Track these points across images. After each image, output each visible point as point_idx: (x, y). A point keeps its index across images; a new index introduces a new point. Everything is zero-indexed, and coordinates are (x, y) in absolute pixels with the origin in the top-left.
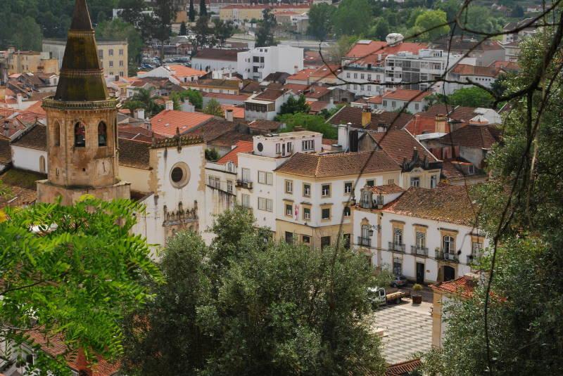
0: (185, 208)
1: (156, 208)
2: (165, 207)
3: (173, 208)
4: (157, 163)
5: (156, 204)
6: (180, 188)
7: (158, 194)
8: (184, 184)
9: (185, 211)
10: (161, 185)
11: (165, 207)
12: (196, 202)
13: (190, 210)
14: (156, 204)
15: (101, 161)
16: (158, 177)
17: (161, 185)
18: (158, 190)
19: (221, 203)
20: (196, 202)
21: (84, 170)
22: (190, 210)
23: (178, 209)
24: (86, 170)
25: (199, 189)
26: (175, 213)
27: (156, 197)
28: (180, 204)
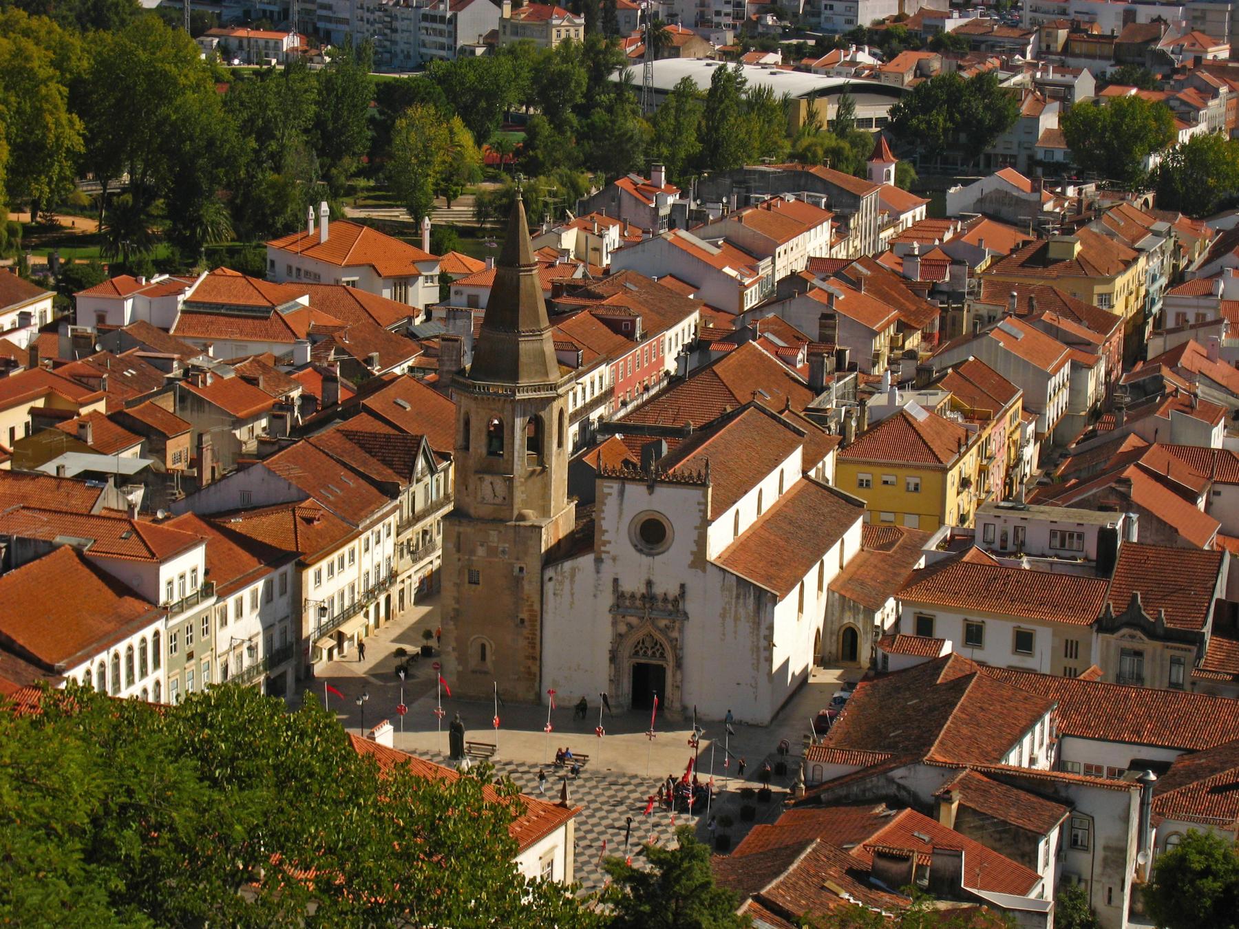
1: (599, 579)
2: (616, 581)
3: (633, 584)
5: (598, 572)
6: (648, 555)
7: (604, 556)
8: (661, 550)
9: (660, 598)
10: (609, 542)
11: (616, 581)
12: (682, 586)
13: (670, 597)
14: (598, 572)
15: (488, 478)
17: (609, 542)
19: (741, 601)
22: (670, 597)
23: (643, 590)
25: (693, 565)
26: (638, 596)
27: (598, 561)
28: (649, 584)
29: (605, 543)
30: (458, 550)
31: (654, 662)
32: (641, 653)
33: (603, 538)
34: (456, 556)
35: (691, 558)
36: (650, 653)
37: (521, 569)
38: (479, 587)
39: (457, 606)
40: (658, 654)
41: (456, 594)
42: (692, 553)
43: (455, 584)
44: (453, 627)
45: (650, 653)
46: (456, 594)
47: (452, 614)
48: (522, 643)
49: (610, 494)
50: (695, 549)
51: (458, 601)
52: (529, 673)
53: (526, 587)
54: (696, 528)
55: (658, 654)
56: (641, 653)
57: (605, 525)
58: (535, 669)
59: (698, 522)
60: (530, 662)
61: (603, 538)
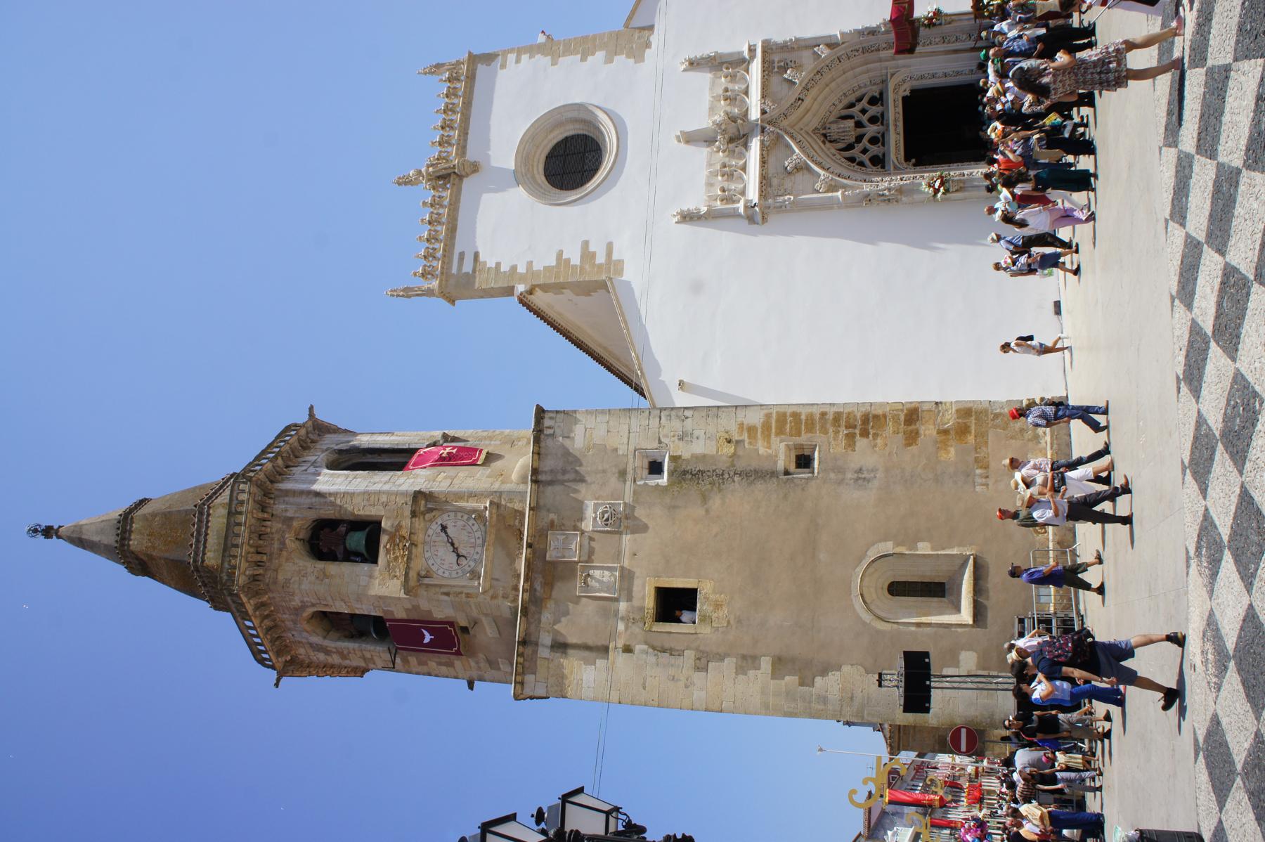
0: (703, 120)
3: (694, 177)
4: (498, 265)
10: (586, 244)
16: (554, 263)
17: (586, 244)
18: (601, 259)
20: (694, 64)
21: (465, 630)
24: (463, 623)
29: (587, 255)
30: (604, 650)
31: (894, 112)
32: (875, 150)
33: (576, 260)
34: (620, 659)
35: (620, 59)
36: (872, 130)
37: (655, 468)
38: (706, 591)
39: (766, 664)
40: (874, 110)
41: (730, 663)
42: (609, 60)
43: (703, 662)
44: (833, 677)
45: (872, 130)
46: (730, 663)
47: (791, 680)
48: (865, 454)
49: (476, 255)
50: (600, 55)
51: (748, 661)
52: (962, 431)
53: (699, 447)
54: (554, 63)
55: (874, 110)
56: (875, 150)
57: (545, 260)
58: (950, 420)
59: (543, 60)
60: (928, 431)
61: (576, 260)
